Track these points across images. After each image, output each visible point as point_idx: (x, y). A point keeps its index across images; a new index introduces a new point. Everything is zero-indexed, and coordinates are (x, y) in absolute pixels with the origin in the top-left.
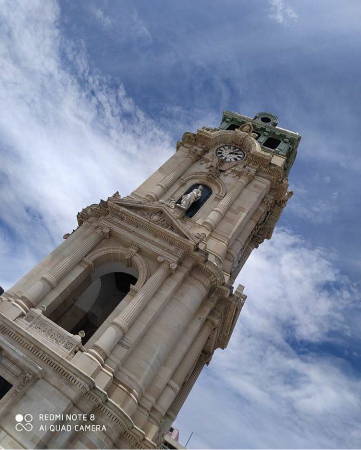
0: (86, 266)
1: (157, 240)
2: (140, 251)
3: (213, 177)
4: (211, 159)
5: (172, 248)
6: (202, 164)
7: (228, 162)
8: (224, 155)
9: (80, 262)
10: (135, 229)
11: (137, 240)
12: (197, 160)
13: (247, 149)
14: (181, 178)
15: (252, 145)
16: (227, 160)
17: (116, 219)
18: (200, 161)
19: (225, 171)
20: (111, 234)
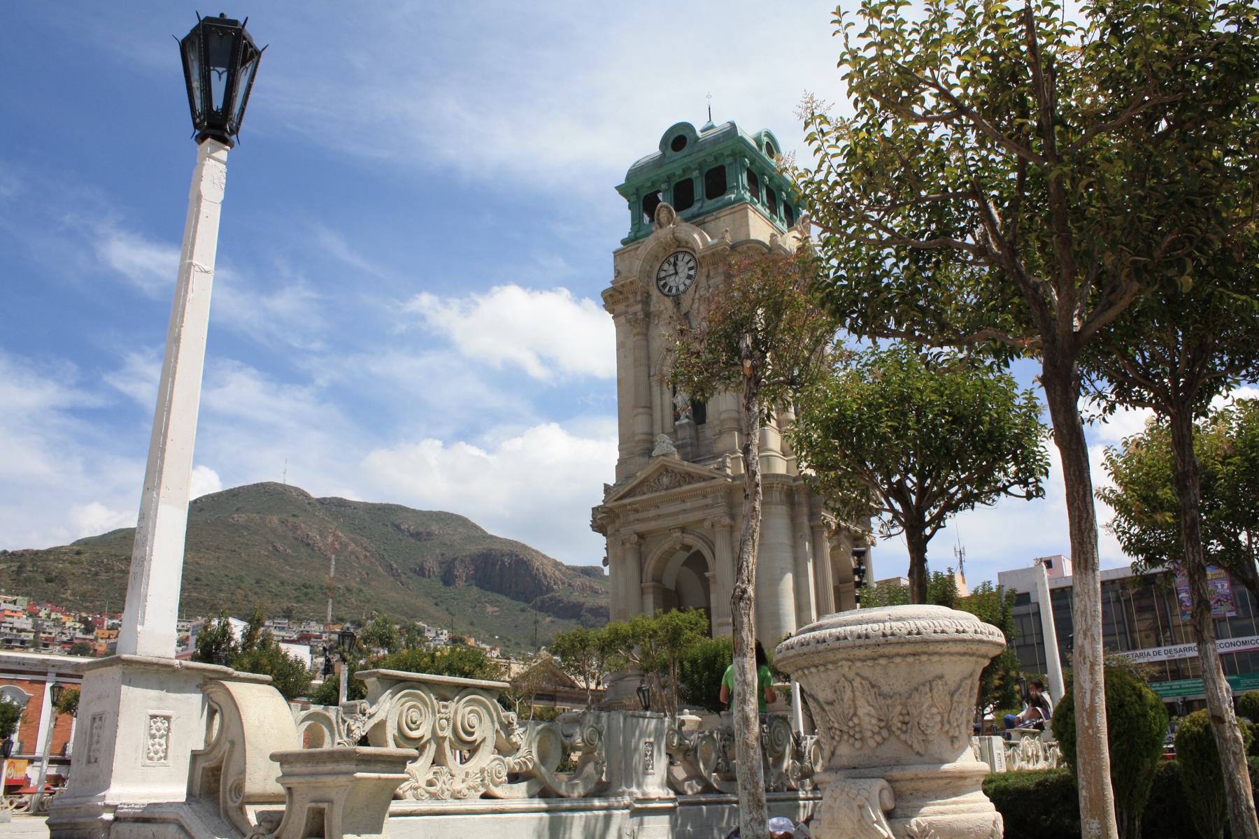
0: (651, 590)
1: (688, 505)
2: (683, 529)
4: (662, 308)
5: (709, 501)
7: (684, 292)
9: (642, 591)
10: (658, 512)
11: (670, 522)
12: (648, 326)
14: (652, 374)
16: (682, 288)
17: (632, 517)
20: (641, 536)
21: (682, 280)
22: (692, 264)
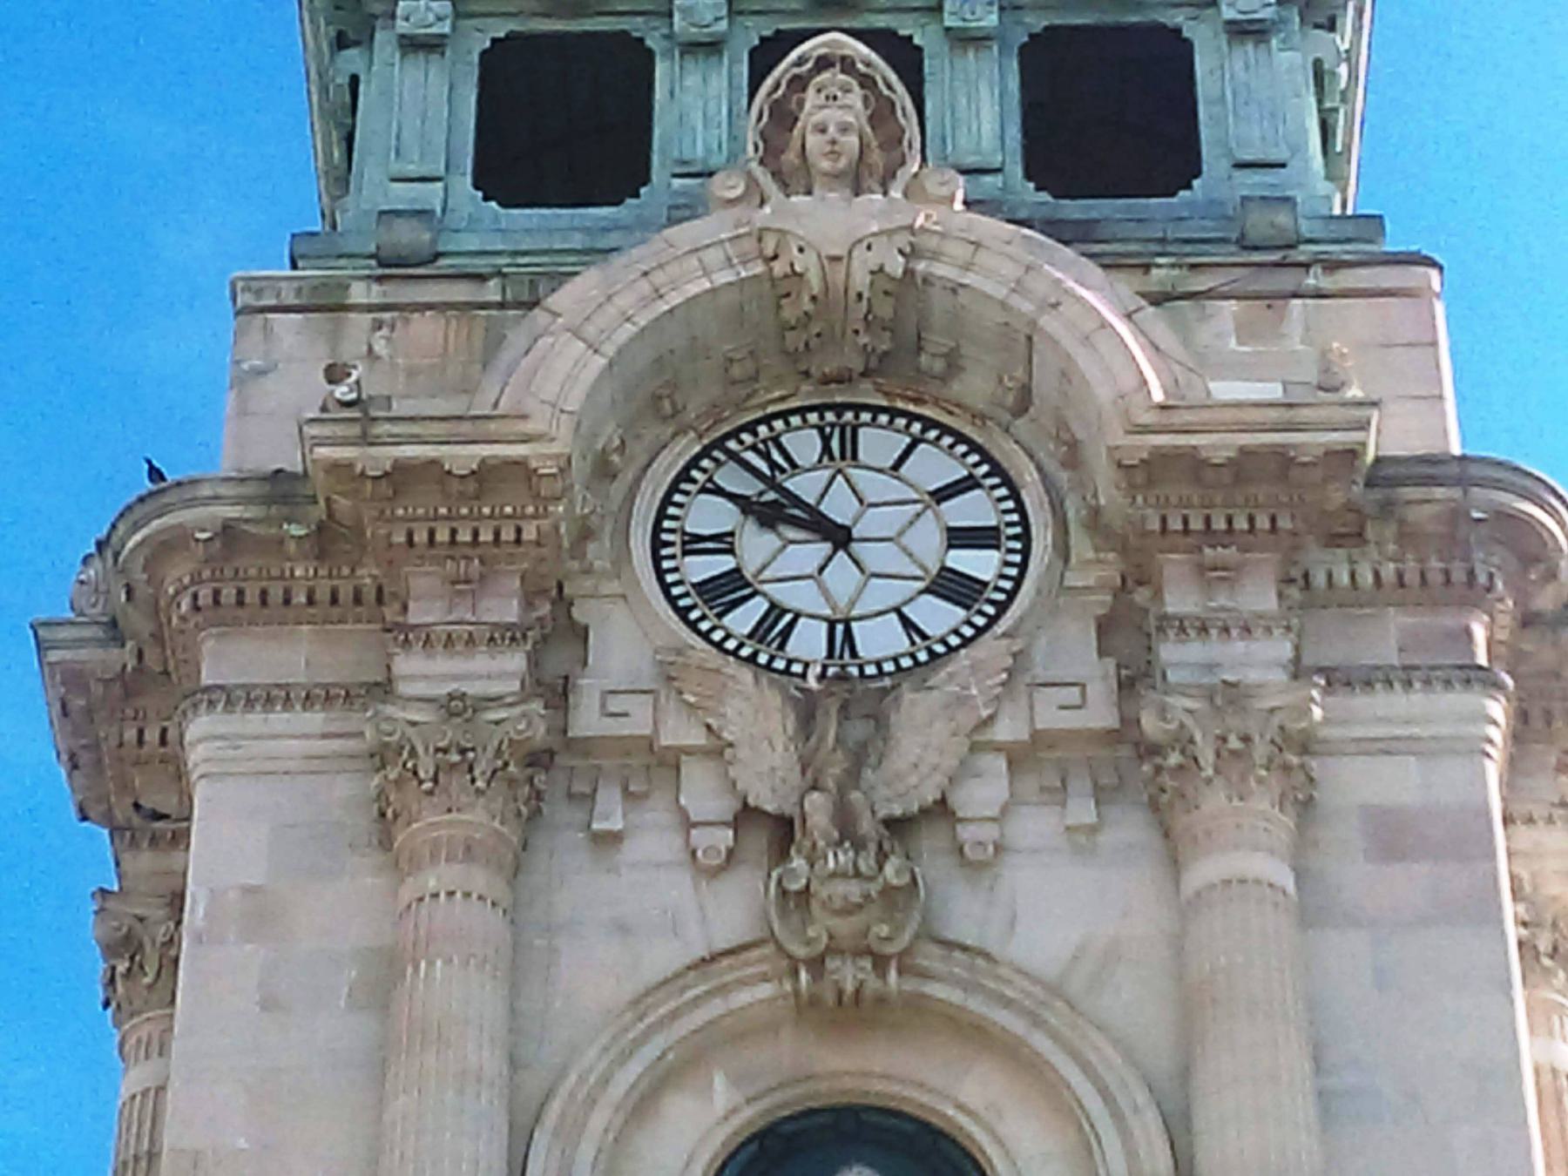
4: (680, 732)
6: (612, 839)
8: (785, 594)
13: (975, 386)
15: (1048, 322)
18: (559, 811)
19: (941, 809)
21: (883, 594)
22: (974, 509)
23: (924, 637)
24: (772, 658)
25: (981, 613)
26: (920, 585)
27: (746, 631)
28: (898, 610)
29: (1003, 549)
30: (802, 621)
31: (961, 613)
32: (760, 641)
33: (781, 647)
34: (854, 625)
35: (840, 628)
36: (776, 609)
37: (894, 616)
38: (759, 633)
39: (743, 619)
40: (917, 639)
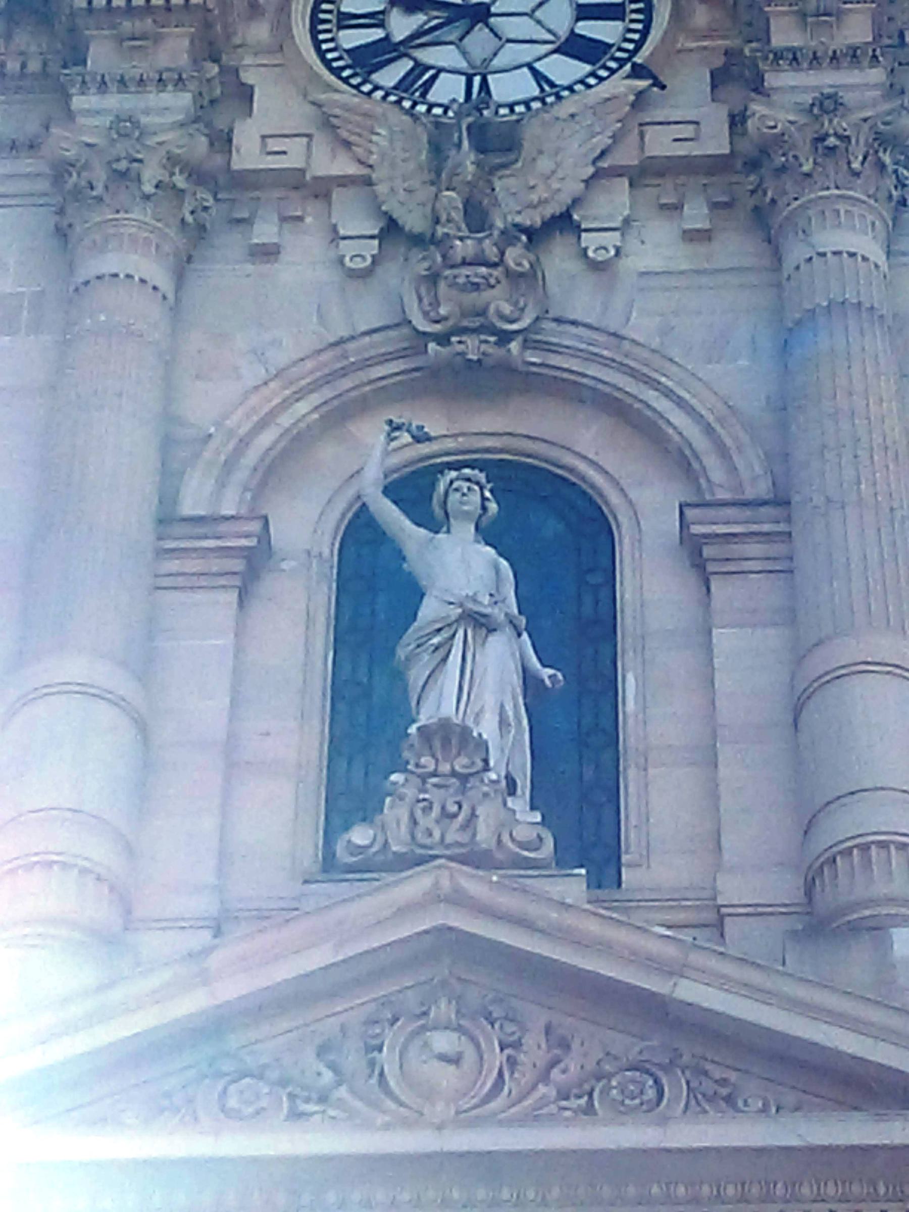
3: (505, 338)
23: (552, 85)
24: (415, 104)
25: (605, 67)
26: (550, 47)
27: (392, 84)
28: (530, 66)
29: (627, 20)
30: (443, 75)
31: (588, 68)
32: (405, 91)
33: (424, 95)
34: (490, 78)
35: (477, 80)
36: (420, 68)
37: (525, 70)
38: (404, 85)
39: (390, 76)
40: (547, 88)
